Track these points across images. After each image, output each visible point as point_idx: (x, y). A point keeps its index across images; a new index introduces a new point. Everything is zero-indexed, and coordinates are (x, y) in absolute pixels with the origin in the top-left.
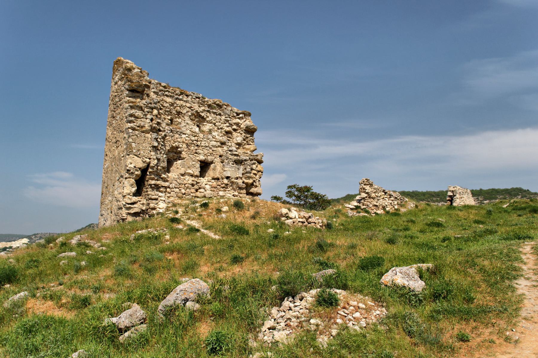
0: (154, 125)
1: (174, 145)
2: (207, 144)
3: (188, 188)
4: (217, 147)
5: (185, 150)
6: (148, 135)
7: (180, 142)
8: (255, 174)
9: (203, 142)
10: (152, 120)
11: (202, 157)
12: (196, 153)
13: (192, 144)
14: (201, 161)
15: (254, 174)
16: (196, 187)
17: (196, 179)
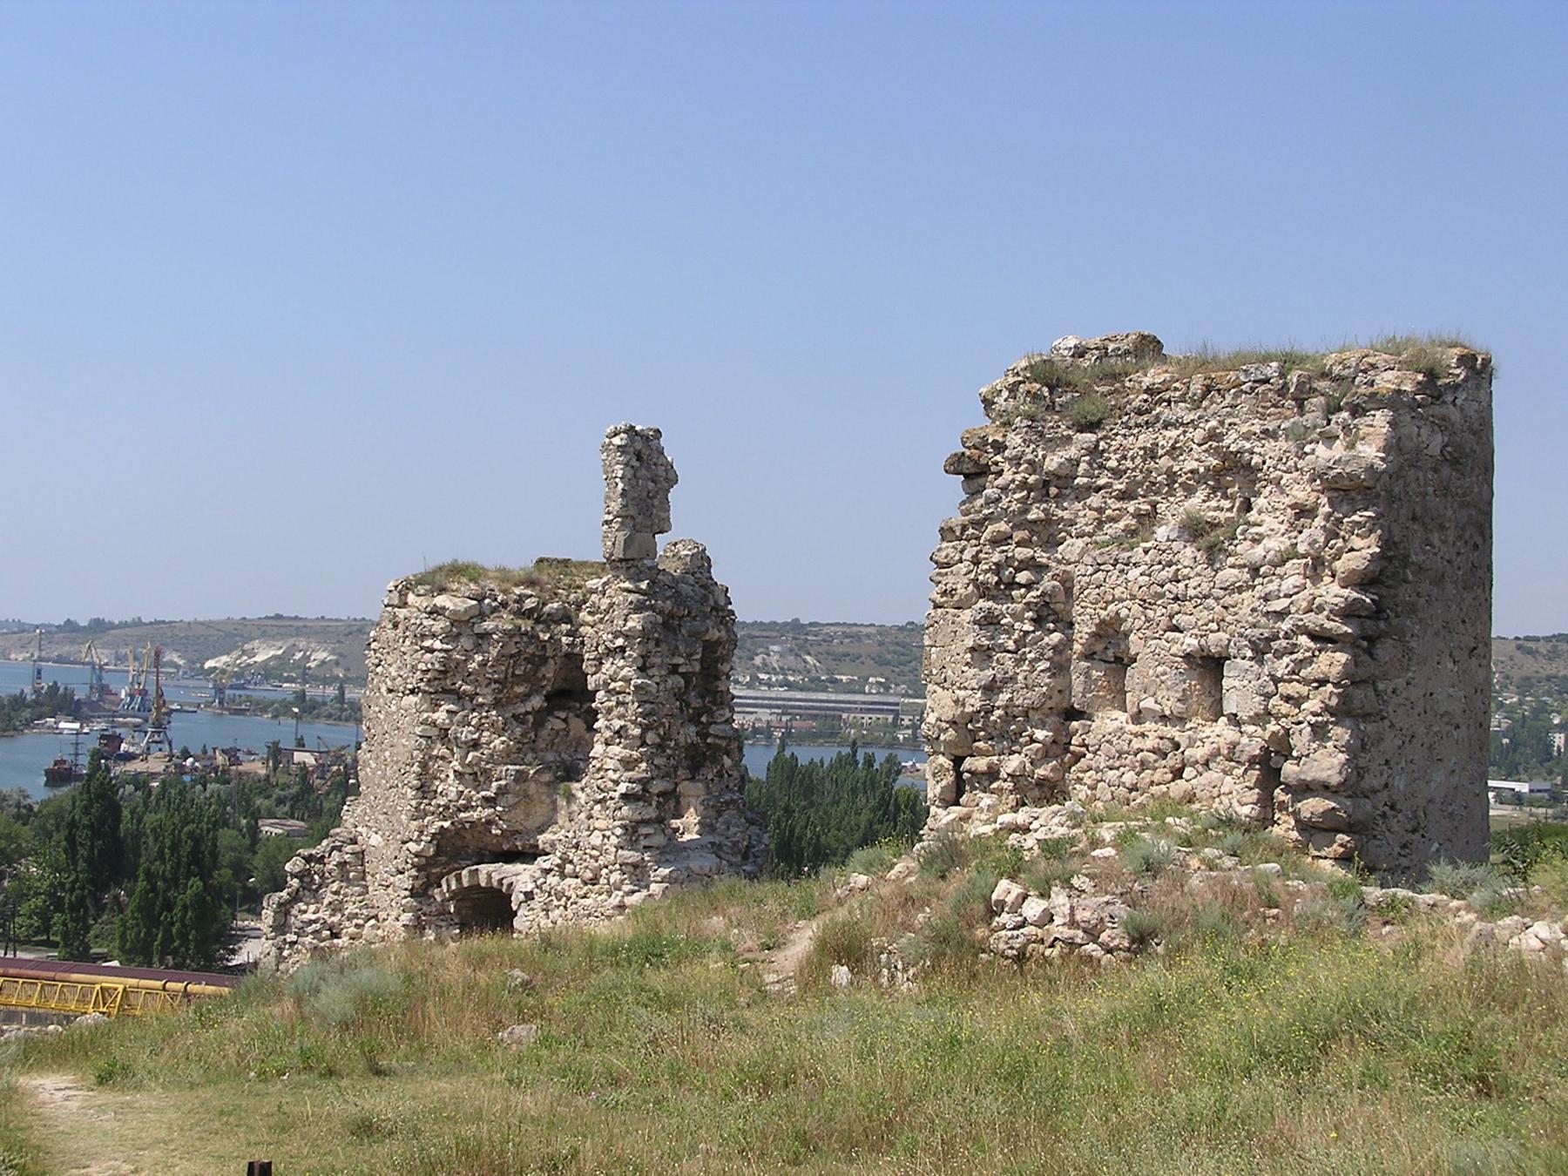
0: (981, 578)
1: (1103, 613)
2: (1205, 588)
3: (1144, 765)
4: (1240, 590)
5: (1138, 624)
6: (966, 615)
7: (1122, 600)
8: (1296, 701)
9: (1193, 583)
10: (976, 561)
11: (1190, 642)
12: (1176, 629)
13: (1162, 596)
14: (1188, 657)
15: (1288, 699)
16: (1173, 760)
17: (1172, 731)
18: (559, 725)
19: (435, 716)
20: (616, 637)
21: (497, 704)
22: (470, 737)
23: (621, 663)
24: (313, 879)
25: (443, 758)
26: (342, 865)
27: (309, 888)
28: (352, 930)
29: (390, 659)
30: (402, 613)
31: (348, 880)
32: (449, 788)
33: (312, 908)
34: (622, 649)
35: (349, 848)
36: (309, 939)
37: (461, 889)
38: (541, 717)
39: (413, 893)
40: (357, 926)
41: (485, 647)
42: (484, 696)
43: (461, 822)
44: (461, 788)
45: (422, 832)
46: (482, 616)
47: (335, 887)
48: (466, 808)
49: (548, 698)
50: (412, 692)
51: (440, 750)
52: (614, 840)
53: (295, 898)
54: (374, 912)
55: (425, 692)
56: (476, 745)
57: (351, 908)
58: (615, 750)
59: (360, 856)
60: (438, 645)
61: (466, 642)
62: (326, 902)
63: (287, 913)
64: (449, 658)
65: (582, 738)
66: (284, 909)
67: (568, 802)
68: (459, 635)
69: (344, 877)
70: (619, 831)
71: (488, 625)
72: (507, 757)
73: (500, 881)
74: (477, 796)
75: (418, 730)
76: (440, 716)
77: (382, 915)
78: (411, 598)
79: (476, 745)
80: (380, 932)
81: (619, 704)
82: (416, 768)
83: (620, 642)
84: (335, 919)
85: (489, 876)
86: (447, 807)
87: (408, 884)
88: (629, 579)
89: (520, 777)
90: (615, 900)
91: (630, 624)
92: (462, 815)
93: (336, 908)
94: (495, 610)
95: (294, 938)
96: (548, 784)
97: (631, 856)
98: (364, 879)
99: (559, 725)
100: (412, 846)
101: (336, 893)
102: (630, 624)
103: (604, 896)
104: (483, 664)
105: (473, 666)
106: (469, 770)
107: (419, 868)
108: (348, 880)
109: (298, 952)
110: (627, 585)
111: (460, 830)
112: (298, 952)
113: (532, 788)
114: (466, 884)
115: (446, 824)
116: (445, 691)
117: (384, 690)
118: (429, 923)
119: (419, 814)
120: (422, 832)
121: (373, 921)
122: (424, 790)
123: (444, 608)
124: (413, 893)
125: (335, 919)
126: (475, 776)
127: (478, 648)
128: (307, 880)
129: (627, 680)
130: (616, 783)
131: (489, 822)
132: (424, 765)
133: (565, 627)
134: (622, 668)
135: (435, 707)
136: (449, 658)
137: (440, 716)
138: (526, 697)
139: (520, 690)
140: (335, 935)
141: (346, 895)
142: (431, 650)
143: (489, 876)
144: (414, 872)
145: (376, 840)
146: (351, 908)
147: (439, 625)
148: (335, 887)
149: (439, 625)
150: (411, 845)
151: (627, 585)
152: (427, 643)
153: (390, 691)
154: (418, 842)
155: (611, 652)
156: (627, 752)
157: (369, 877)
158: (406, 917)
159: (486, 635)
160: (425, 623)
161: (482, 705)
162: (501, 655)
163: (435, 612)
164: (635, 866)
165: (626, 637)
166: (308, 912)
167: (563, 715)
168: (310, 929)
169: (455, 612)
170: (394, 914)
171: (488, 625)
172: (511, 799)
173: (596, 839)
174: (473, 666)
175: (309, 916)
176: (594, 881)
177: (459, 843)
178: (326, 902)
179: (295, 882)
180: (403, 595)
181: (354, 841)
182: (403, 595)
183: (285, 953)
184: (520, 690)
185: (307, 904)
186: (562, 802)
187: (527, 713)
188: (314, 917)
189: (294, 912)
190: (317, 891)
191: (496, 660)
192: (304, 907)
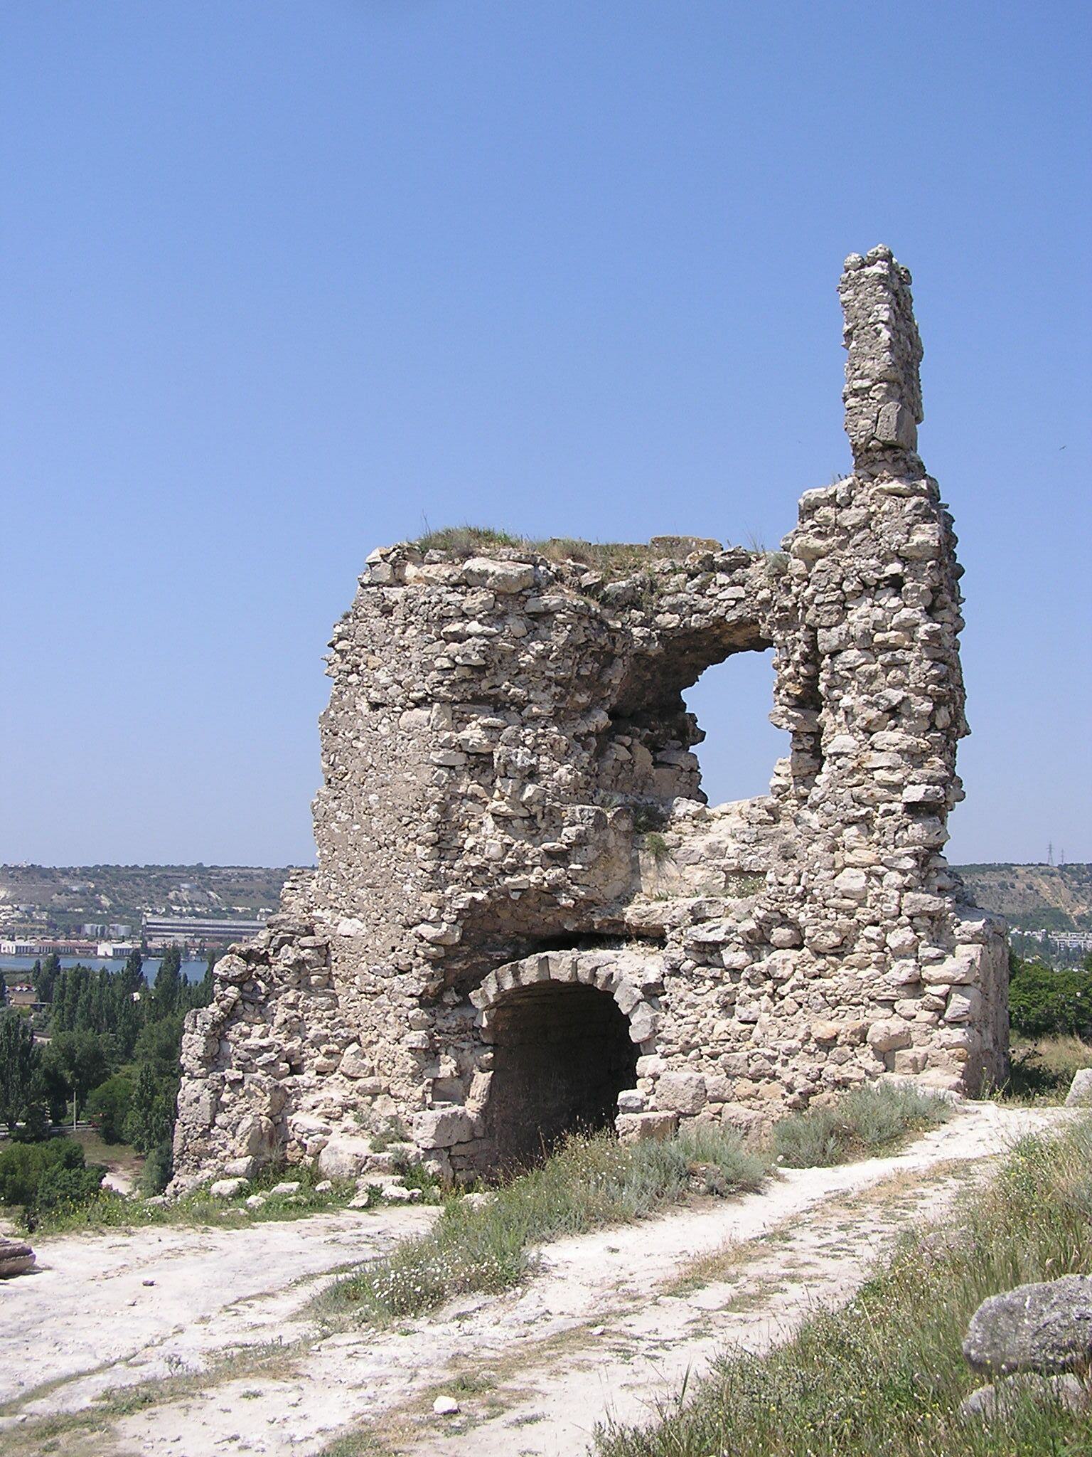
18: (623, 754)
19: (465, 734)
20: (886, 562)
21: (557, 717)
22: (528, 762)
23: (895, 602)
24: (256, 987)
25: (474, 798)
26: (300, 964)
27: (252, 1001)
28: (320, 1060)
29: (375, 661)
30: (396, 594)
31: (308, 987)
32: (486, 839)
33: (258, 1030)
34: (896, 583)
35: (306, 941)
36: (259, 1074)
37: (520, 990)
38: (606, 737)
39: (425, 1001)
40: (329, 1054)
41: (543, 632)
42: (539, 704)
43: (506, 892)
44: (507, 841)
45: (442, 909)
46: (538, 588)
47: (291, 997)
48: (514, 870)
49: (612, 715)
50: (419, 703)
51: (467, 785)
52: (894, 878)
53: (232, 1015)
54: (354, 1032)
55: (444, 701)
56: (532, 774)
57: (315, 1029)
58: (887, 737)
59: (324, 950)
60: (474, 627)
61: (516, 626)
62: (279, 1019)
63: (223, 1038)
64: (492, 647)
65: (648, 775)
66: (218, 1033)
67: (659, 859)
68: (505, 613)
69: (303, 984)
70: (909, 863)
71: (550, 600)
72: (583, 791)
73: (593, 973)
74: (533, 851)
75: (436, 757)
76: (473, 734)
77: (366, 1037)
78: (411, 571)
79: (532, 774)
80: (366, 1061)
81: (887, 667)
82: (433, 813)
83: (895, 568)
84: (295, 1045)
85: (575, 966)
86: (481, 870)
87: (417, 987)
88: (899, 477)
89: (599, 822)
90: (901, 971)
91: (917, 538)
92: (508, 879)
93: (294, 1028)
94: (550, 582)
95: (238, 1074)
96: (626, 834)
97: (929, 901)
98: (329, 985)
99: (623, 754)
100: (427, 931)
101: (293, 1006)
102: (917, 538)
103: (871, 970)
104: (542, 657)
105: (526, 659)
106: (524, 813)
107: (435, 962)
108: (308, 987)
109: (250, 1094)
110: (895, 484)
111: (502, 900)
112: (250, 1094)
113: (612, 839)
114: (525, 982)
115: (480, 896)
116: (477, 700)
117: (363, 706)
118: (446, 1045)
119: (436, 881)
120: (442, 909)
121: (354, 1047)
122: (443, 846)
123: (485, 574)
124: (425, 1001)
125: (295, 1045)
126: (536, 821)
127: (533, 634)
128: (248, 987)
129: (909, 628)
130: (898, 787)
131: (556, 888)
132: (444, 809)
133: (636, 614)
134: (896, 610)
135: (461, 722)
136: (492, 647)
137: (473, 734)
138: (586, 711)
139: (583, 699)
140: (296, 1070)
141: (306, 1009)
142: (459, 638)
143: (575, 966)
144: (428, 969)
145: (348, 926)
146: (315, 1029)
147: (476, 600)
148: (291, 997)
149: (476, 600)
150: (425, 930)
151: (895, 484)
152: (455, 627)
153: (375, 706)
154: (435, 923)
155: (867, 589)
156: (911, 740)
157: (337, 983)
158: (416, 1038)
159: (548, 613)
160: (450, 598)
161: (535, 718)
162: (571, 646)
163: (465, 583)
164: (931, 916)
165: (904, 560)
166: (252, 1035)
167: (627, 740)
168: (260, 1061)
169: (505, 578)
170: (392, 1033)
171: (550, 600)
172: (591, 853)
173: (852, 880)
174: (526, 659)
175: (253, 1042)
176: (840, 951)
177: (489, 926)
178: (279, 1019)
179: (232, 992)
180: (397, 566)
181: (310, 932)
182: (397, 566)
183: (225, 1098)
184: (583, 699)
185: (250, 1024)
186: (646, 859)
187: (590, 734)
188: (264, 1042)
189: (232, 1036)
190: (263, 1004)
191: (563, 650)
192: (246, 1029)
